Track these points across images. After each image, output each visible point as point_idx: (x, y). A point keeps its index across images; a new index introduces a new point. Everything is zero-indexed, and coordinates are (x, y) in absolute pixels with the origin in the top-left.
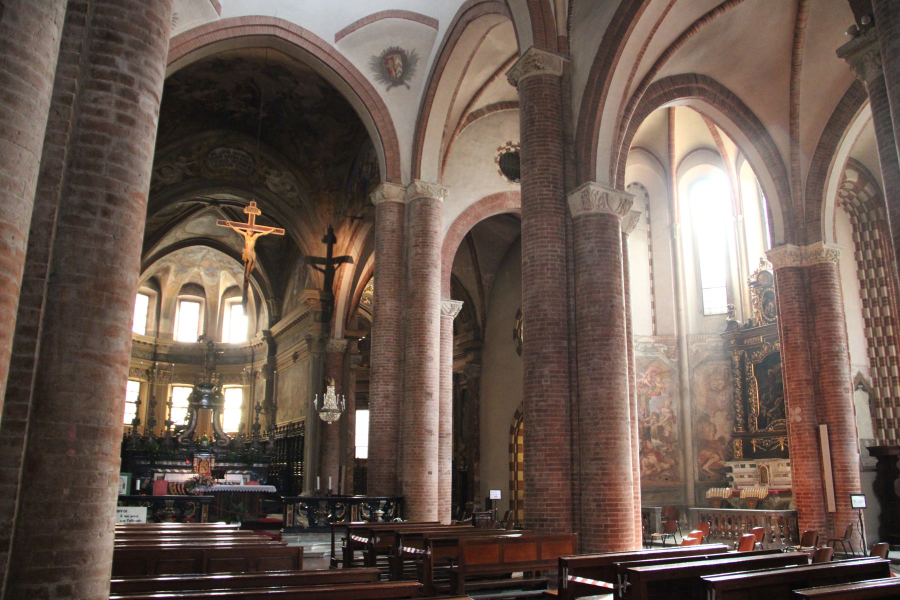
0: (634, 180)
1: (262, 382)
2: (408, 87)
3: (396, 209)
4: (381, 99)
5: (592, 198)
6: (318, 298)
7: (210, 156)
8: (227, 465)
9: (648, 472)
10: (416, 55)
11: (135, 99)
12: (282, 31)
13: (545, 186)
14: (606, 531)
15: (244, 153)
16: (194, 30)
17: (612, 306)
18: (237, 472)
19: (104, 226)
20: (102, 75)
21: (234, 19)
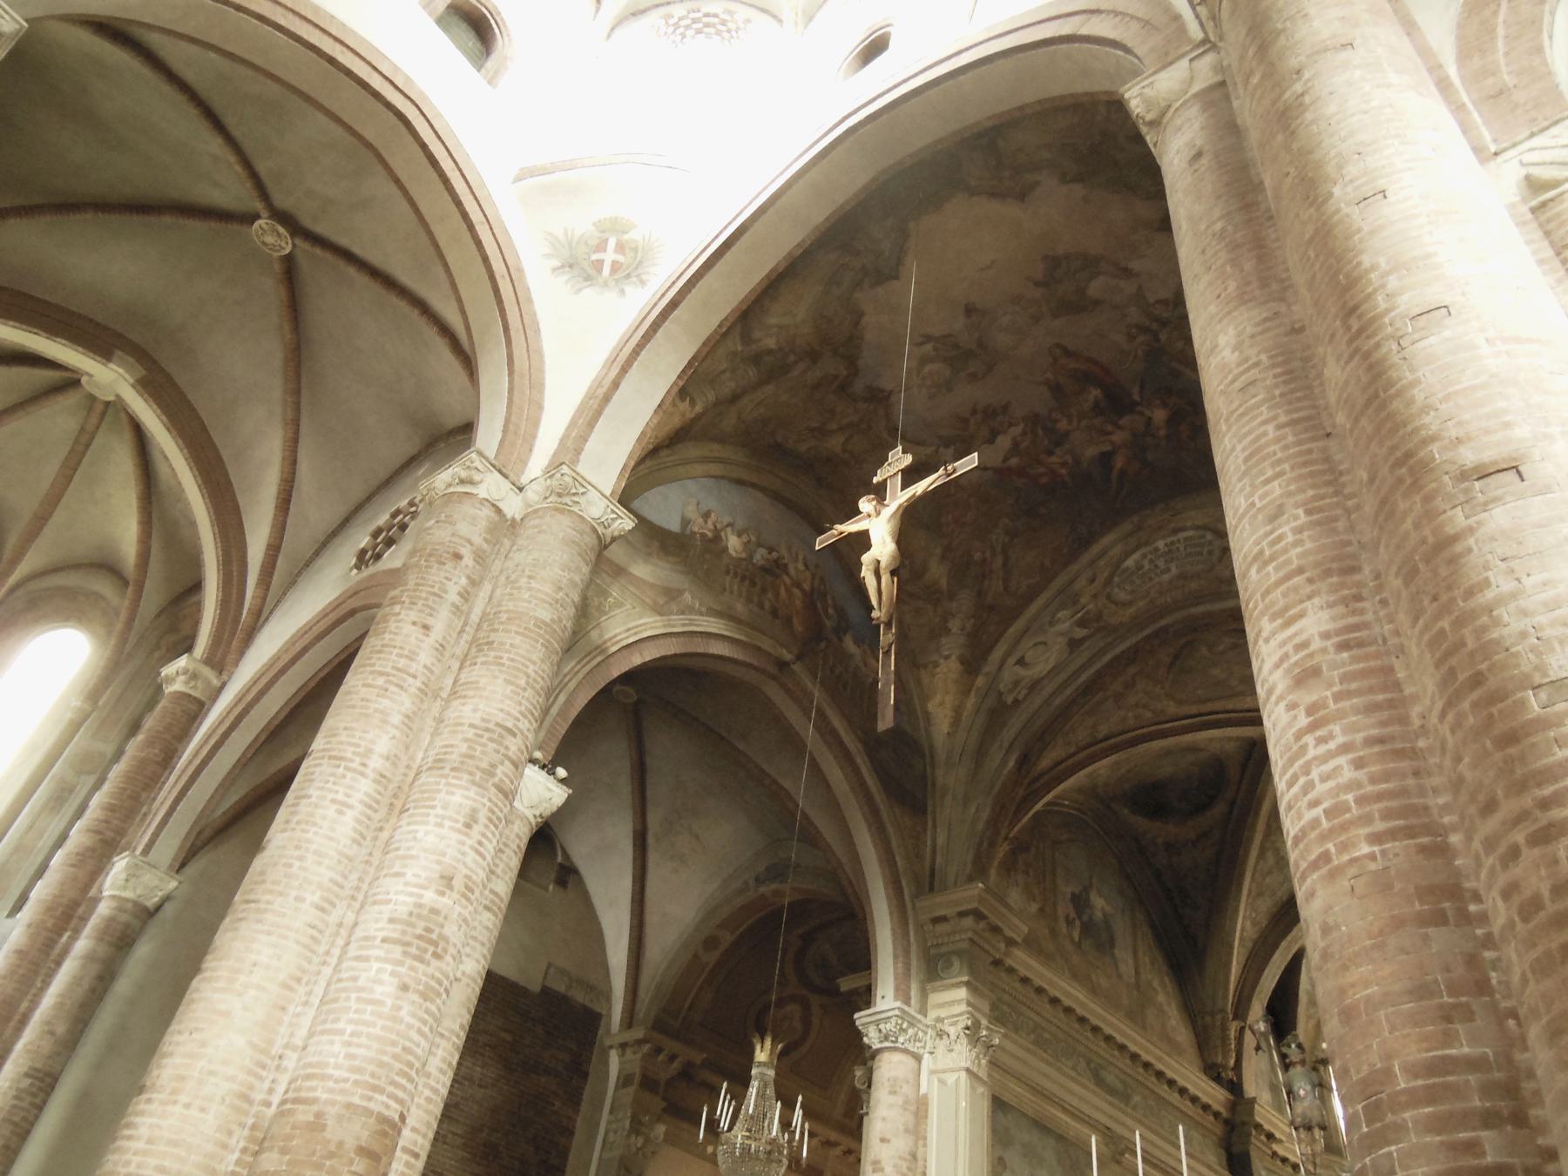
7: (1116, 579)
15: (1190, 533)
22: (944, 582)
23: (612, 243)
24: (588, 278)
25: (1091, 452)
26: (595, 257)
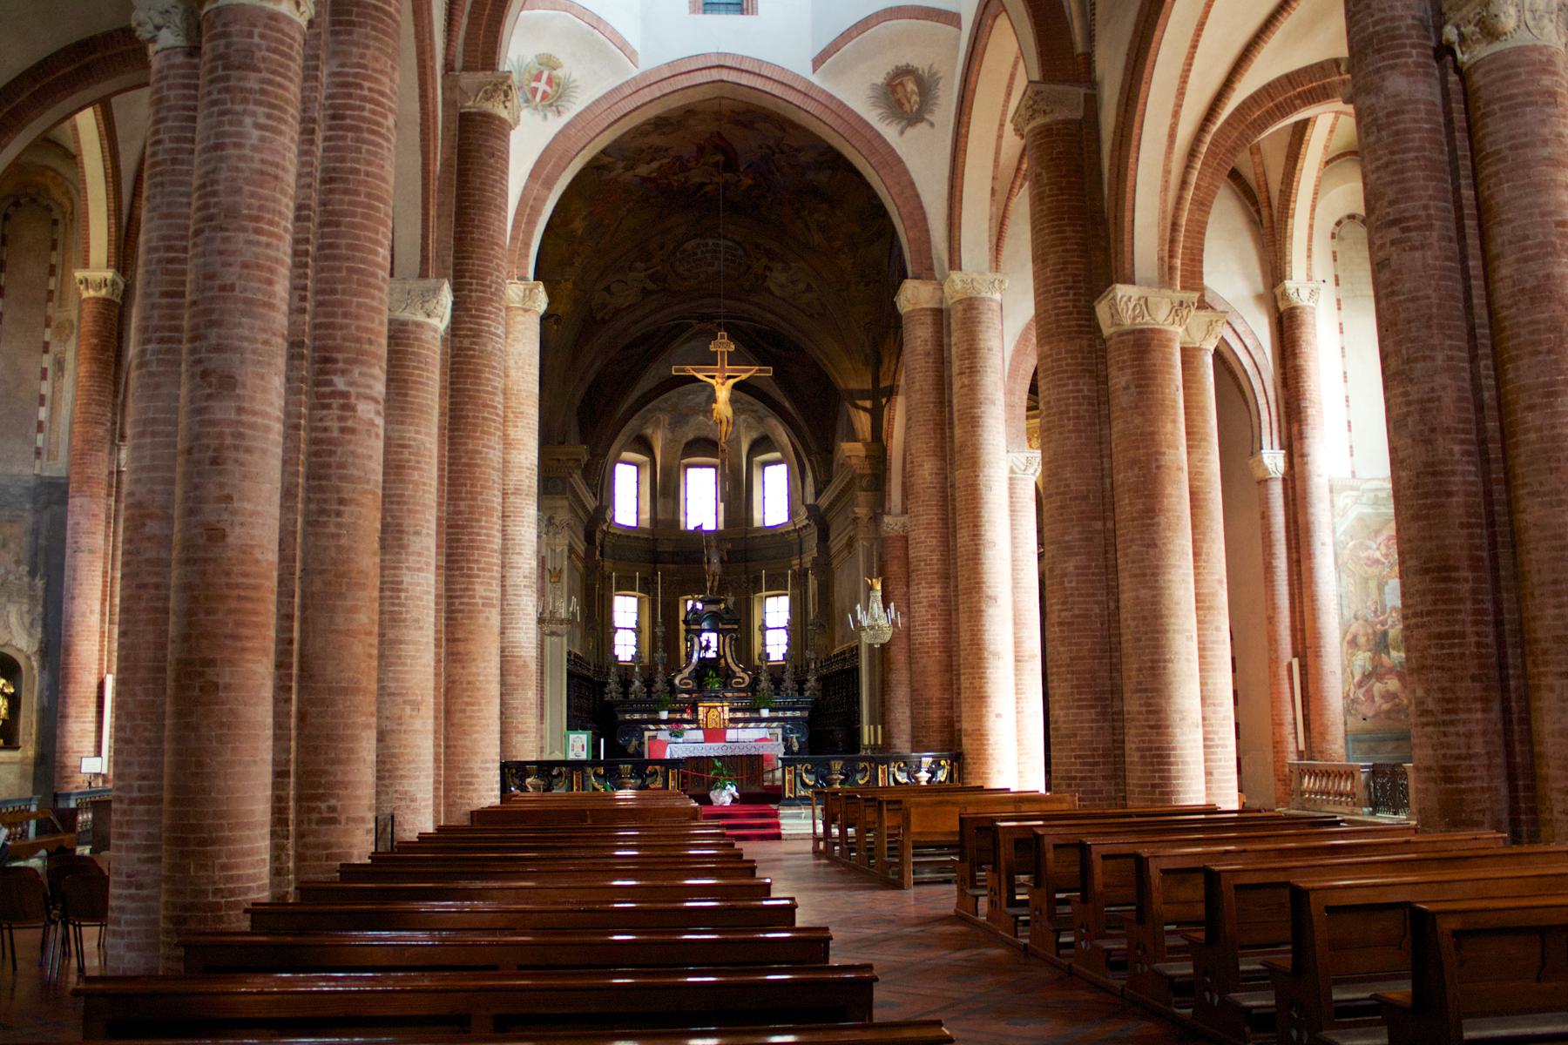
0: (1348, 212)
1: (812, 584)
2: (932, 125)
3: (929, 319)
4: (893, 150)
5: (1121, 306)
6: (863, 453)
8: (645, 716)
9: (1385, 707)
10: (936, 73)
11: (353, 409)
12: (732, 72)
13: (1062, 295)
14: (1153, 793)
15: (730, 244)
16: (604, 97)
17: (1158, 467)
18: (763, 725)
19: (339, 525)
20: (324, 396)
21: (659, 69)
22: (580, 232)
25: (698, 180)
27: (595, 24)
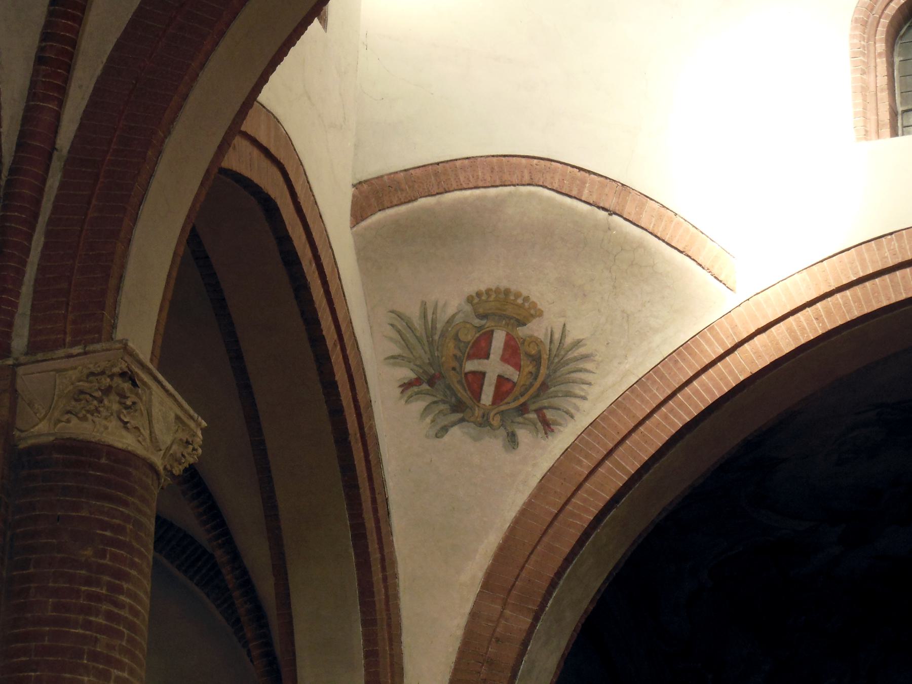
23: (499, 339)
24: (458, 407)
26: (487, 396)
27: (611, 203)
